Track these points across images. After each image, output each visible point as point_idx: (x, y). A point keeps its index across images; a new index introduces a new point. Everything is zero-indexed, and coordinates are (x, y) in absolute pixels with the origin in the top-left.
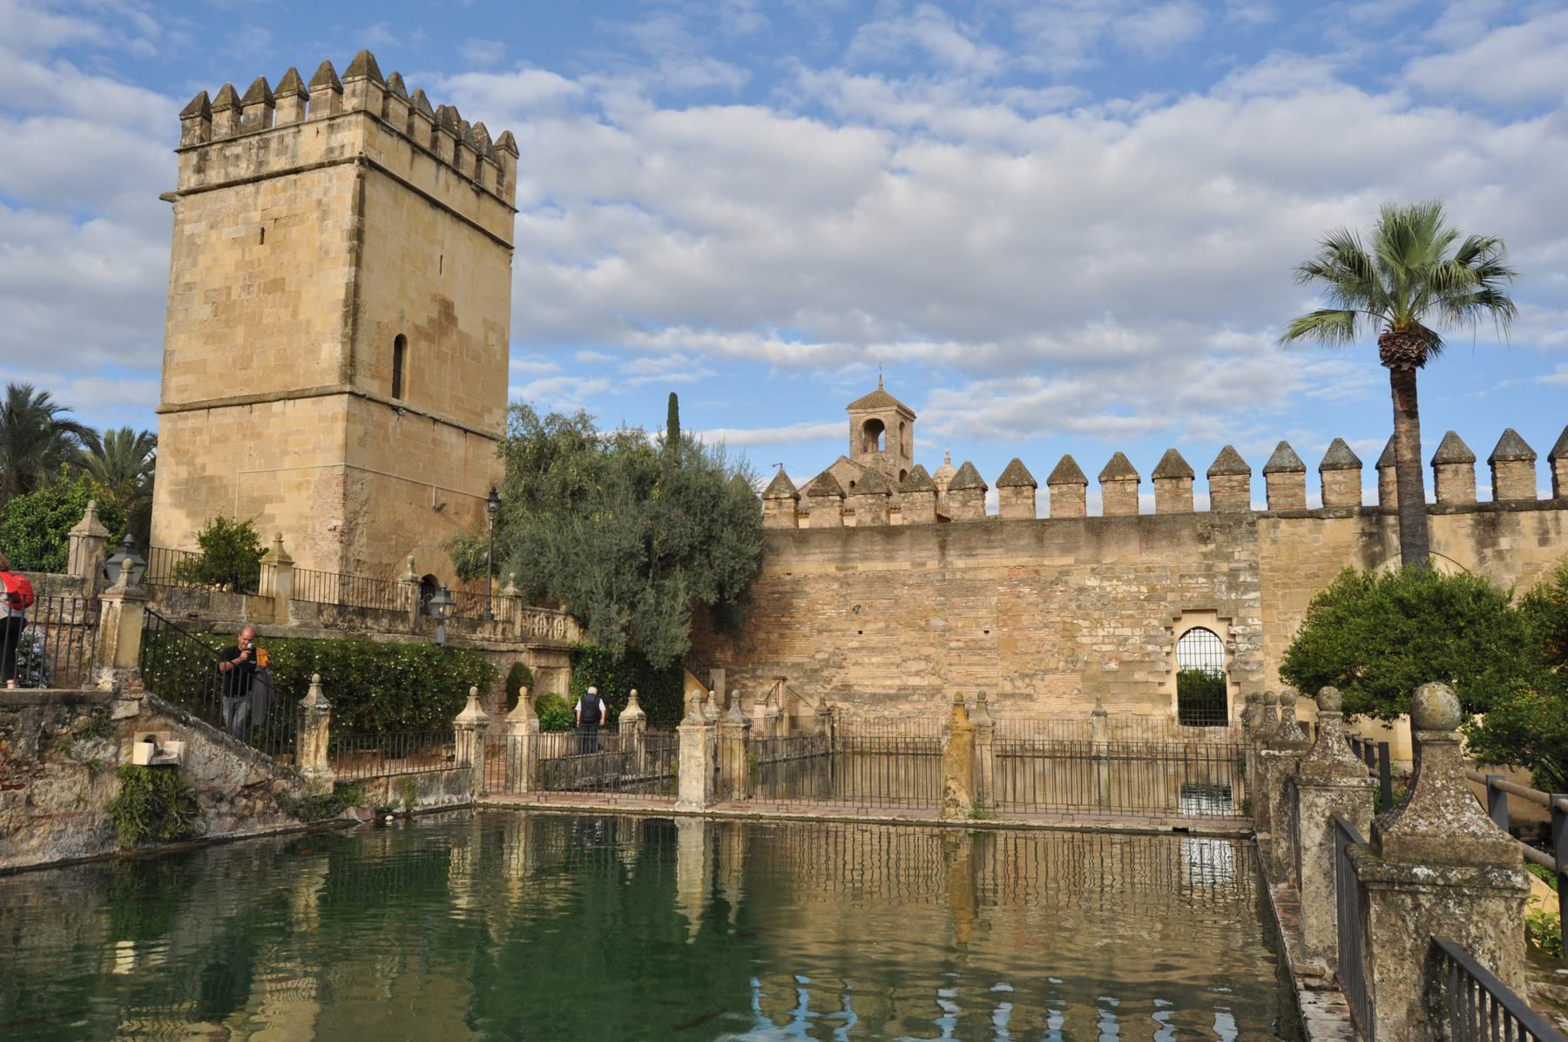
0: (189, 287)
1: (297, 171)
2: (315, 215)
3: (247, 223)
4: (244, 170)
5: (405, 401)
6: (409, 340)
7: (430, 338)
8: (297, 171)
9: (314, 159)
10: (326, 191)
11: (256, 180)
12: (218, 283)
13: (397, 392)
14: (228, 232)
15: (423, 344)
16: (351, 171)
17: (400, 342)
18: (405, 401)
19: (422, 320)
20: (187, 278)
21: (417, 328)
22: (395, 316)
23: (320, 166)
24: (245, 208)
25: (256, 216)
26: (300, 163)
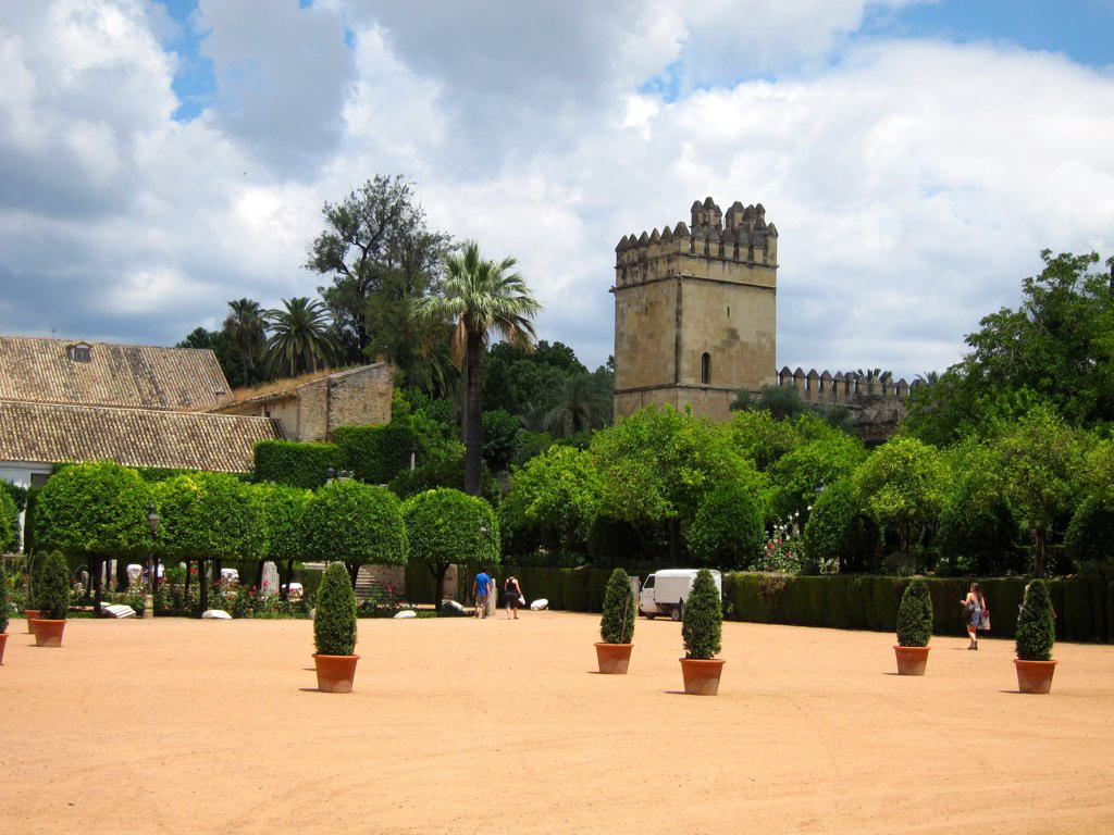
0: (622, 334)
1: (657, 281)
2: (664, 302)
3: (641, 304)
5: (714, 384)
6: (711, 353)
8: (657, 281)
9: (663, 276)
12: (632, 333)
13: (706, 377)
14: (635, 308)
15: (719, 354)
16: (675, 282)
17: (706, 356)
18: (714, 384)
19: (718, 342)
21: (716, 349)
22: (701, 344)
23: (665, 279)
25: (644, 301)
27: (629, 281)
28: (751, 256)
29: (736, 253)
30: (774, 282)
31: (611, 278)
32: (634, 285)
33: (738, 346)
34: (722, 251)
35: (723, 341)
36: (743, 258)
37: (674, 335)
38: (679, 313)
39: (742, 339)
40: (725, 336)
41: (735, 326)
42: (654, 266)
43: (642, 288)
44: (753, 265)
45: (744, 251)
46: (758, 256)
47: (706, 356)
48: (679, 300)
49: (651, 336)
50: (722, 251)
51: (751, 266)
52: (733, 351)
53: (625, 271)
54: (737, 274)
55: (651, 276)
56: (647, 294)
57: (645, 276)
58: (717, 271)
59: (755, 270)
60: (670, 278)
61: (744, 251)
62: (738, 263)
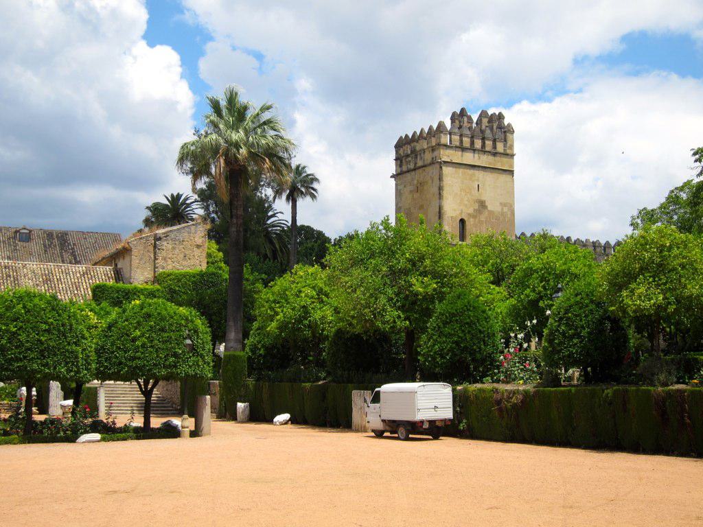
0: (400, 208)
2: (430, 182)
4: (412, 166)
6: (466, 219)
7: (474, 217)
9: (429, 162)
10: (433, 173)
11: (414, 170)
12: (407, 207)
14: (409, 188)
16: (437, 166)
19: (471, 211)
20: (400, 205)
21: (469, 214)
22: (458, 212)
23: (430, 164)
24: (413, 180)
25: (416, 182)
26: (426, 163)
27: (404, 168)
28: (495, 147)
29: (483, 145)
30: (512, 166)
31: (392, 168)
32: (408, 171)
33: (486, 213)
34: (472, 143)
35: (474, 210)
36: (487, 149)
37: (438, 205)
38: (440, 189)
39: (490, 208)
40: (476, 206)
41: (483, 199)
42: (422, 155)
43: (413, 173)
44: (496, 153)
45: (489, 143)
46: (500, 147)
47: (462, 221)
48: (440, 179)
49: (421, 207)
50: (472, 143)
51: (495, 154)
52: (483, 218)
53: (401, 162)
54: (484, 160)
55: (420, 163)
56: (417, 176)
57: (416, 164)
58: (469, 158)
59: (498, 158)
60: (433, 163)
61: (489, 143)
62: (485, 152)
